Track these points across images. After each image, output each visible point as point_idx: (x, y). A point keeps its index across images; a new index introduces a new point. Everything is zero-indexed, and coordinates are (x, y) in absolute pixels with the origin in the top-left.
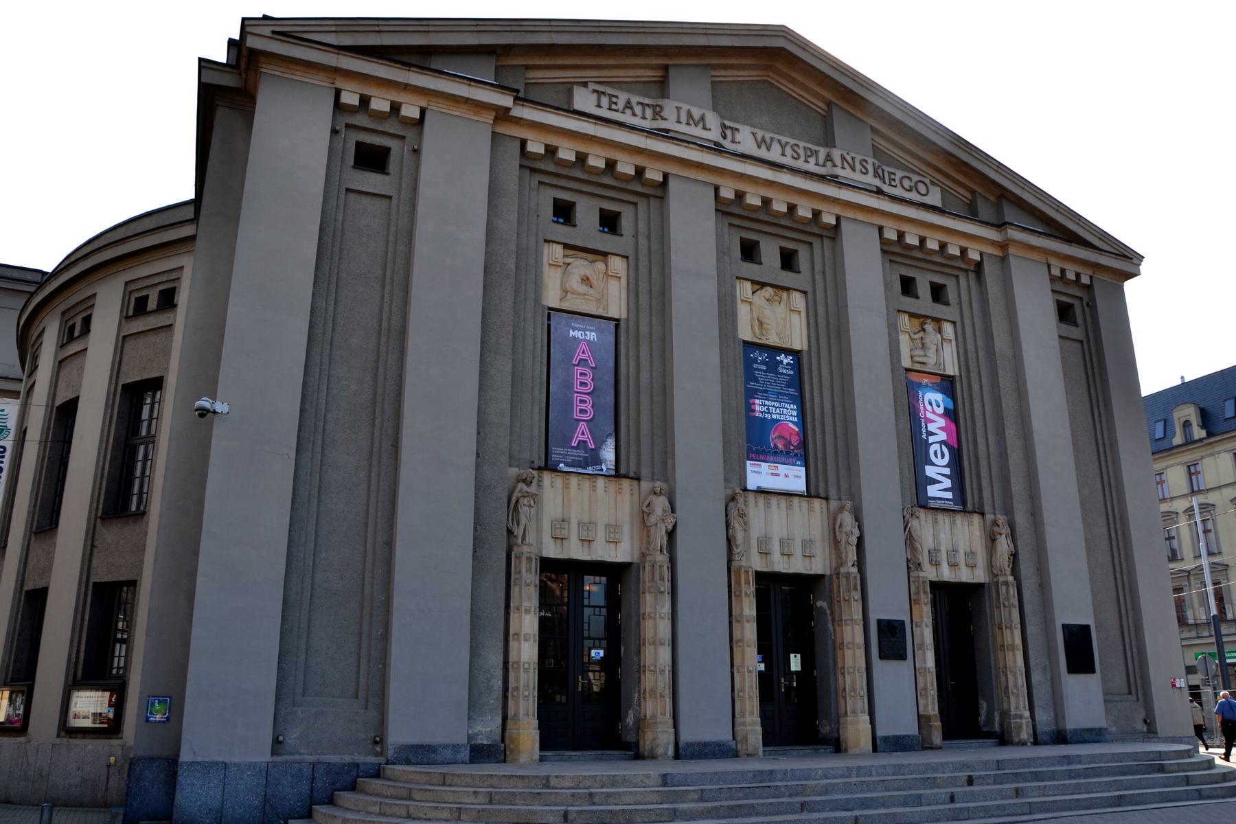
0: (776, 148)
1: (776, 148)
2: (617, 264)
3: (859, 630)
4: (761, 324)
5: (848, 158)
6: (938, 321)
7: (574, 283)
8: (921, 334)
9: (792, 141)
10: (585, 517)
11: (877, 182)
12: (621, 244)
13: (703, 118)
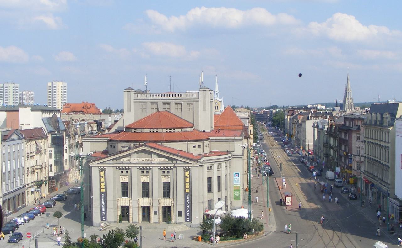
2: (128, 176)
4: (144, 179)
6: (168, 176)
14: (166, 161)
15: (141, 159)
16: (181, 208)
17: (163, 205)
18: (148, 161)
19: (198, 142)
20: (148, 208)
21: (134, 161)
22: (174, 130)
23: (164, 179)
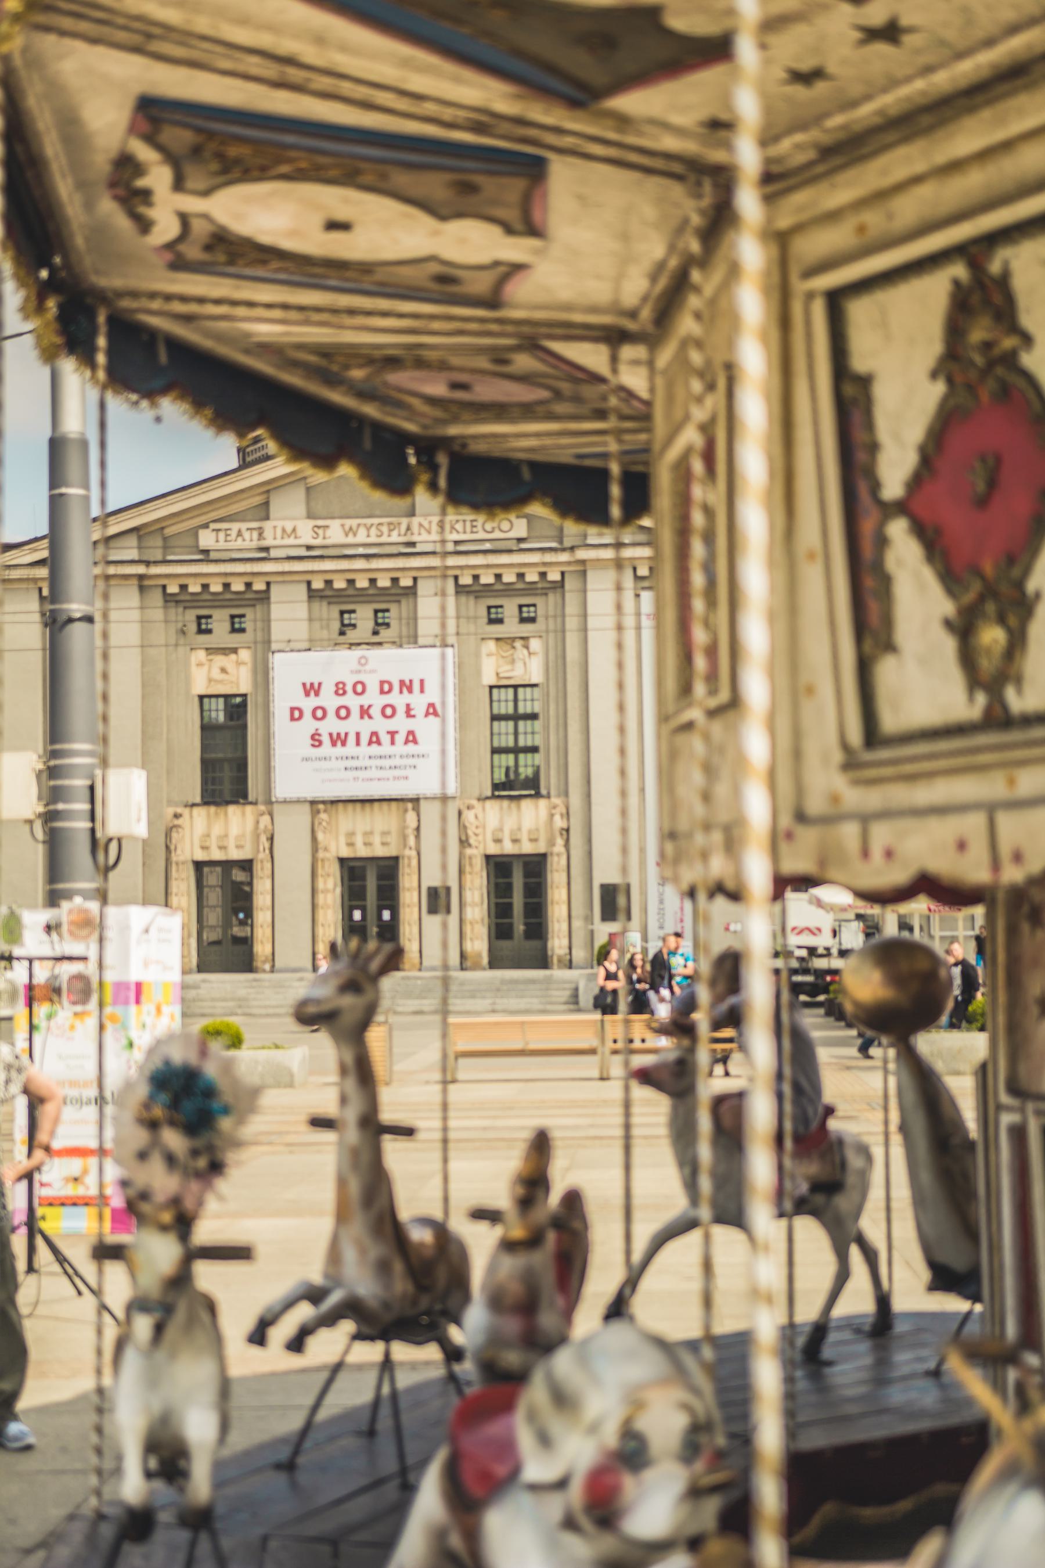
0: (362, 532)
1: (362, 532)
2: (245, 655)
3: (416, 894)
5: (426, 524)
6: (525, 639)
7: (216, 674)
8: (511, 652)
9: (376, 521)
12: (248, 636)
13: (294, 530)
14: (513, 534)
15: (335, 525)
17: (493, 849)
18: (384, 539)
20: (388, 870)
21: (291, 541)
23: (491, 666)
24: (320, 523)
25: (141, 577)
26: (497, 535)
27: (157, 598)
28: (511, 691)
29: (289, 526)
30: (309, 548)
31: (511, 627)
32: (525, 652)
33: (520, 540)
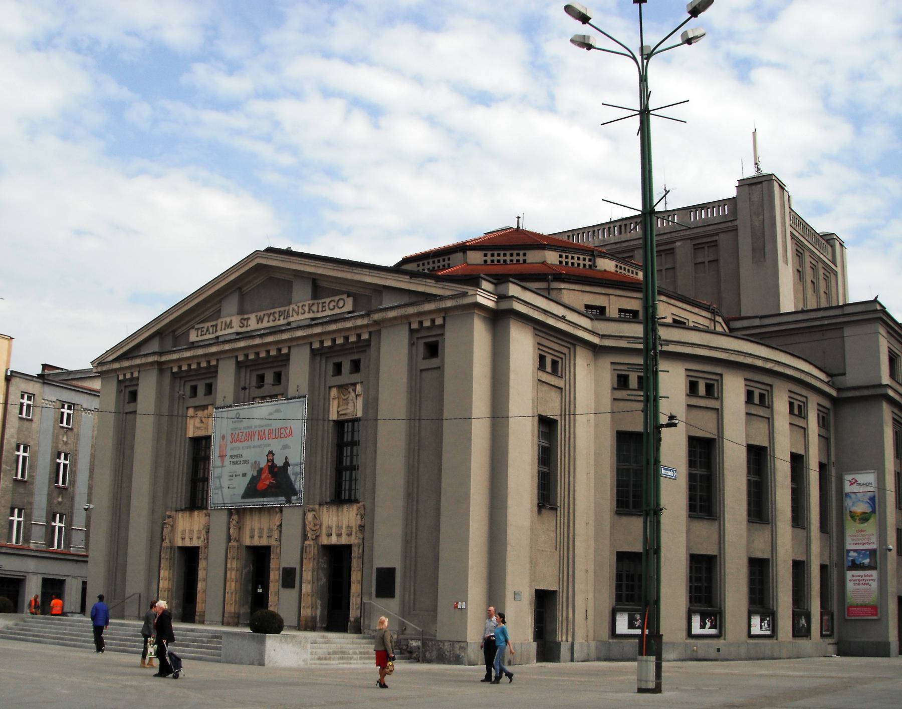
0: (266, 319)
5: (296, 308)
7: (198, 424)
10: (188, 529)
11: (312, 315)
14: (344, 310)
15: (253, 317)
16: (387, 551)
18: (277, 323)
19: (619, 292)
22: (521, 258)
24: (246, 316)
25: (160, 364)
26: (337, 311)
27: (168, 375)
28: (350, 424)
29: (228, 320)
30: (238, 334)
31: (346, 377)
32: (353, 394)
33: (349, 313)
